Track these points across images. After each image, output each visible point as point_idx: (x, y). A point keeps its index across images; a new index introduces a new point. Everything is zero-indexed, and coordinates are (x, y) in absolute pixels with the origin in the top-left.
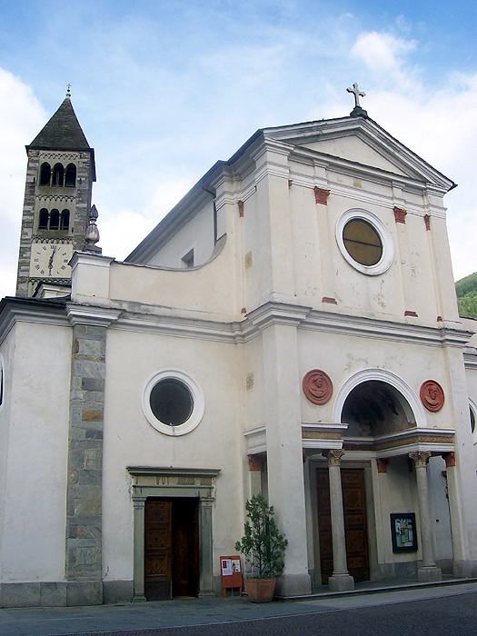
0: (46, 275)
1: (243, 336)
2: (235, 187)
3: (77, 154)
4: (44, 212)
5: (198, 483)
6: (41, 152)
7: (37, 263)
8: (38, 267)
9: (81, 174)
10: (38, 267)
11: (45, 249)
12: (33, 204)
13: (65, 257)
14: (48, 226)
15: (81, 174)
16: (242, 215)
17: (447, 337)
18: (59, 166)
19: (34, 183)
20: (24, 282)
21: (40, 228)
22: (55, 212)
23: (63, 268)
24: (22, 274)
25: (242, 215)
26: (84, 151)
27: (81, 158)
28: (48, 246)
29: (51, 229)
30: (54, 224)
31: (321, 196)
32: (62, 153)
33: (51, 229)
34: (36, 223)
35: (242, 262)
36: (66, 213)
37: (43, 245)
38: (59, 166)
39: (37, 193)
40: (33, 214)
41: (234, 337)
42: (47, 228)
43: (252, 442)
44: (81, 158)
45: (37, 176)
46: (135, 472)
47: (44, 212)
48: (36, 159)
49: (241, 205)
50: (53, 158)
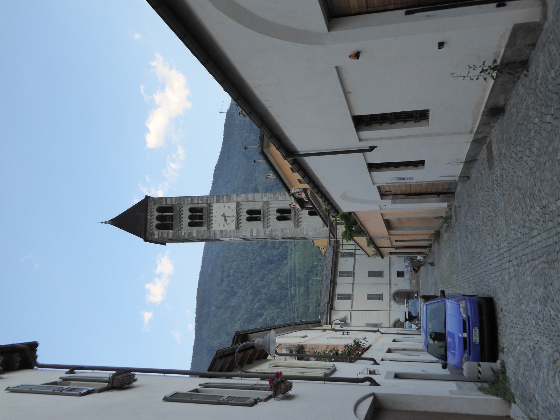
0: (234, 219)
4: (191, 225)
11: (216, 221)
13: (222, 207)
18: (158, 218)
22: (190, 217)
23: (229, 207)
28: (214, 219)
30: (201, 217)
36: (191, 210)
37: (214, 222)
38: (158, 218)
47: (191, 225)
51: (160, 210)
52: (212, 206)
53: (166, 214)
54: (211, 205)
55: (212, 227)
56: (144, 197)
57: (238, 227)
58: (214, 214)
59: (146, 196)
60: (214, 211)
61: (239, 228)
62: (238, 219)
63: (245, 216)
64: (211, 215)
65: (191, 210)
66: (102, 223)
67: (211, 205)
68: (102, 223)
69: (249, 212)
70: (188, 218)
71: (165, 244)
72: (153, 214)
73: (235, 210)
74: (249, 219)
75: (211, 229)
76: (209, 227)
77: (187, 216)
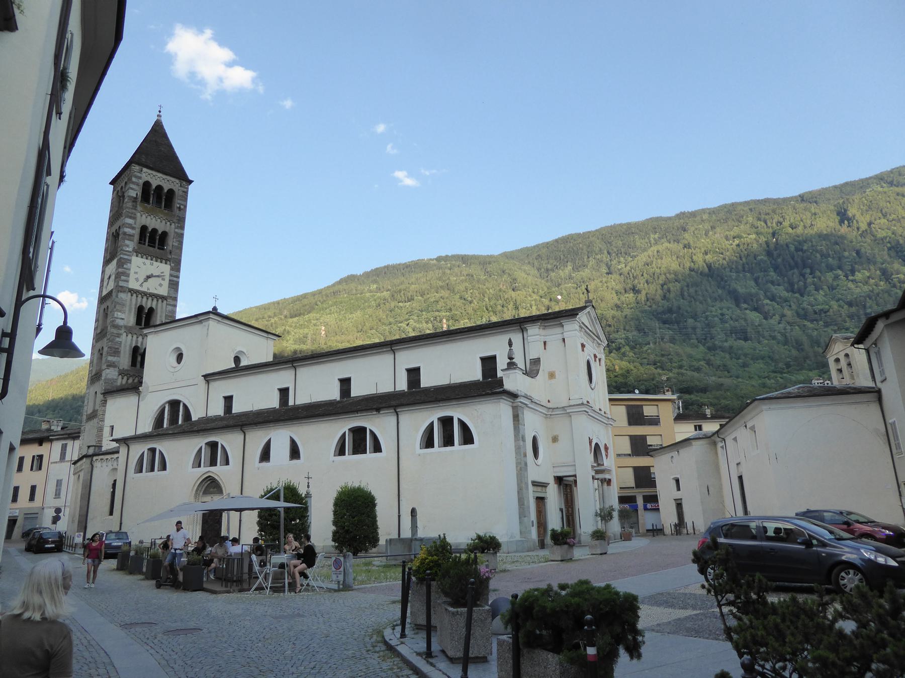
1: (551, 415)
2: (542, 332)
3: (177, 181)
4: (144, 228)
5: (544, 488)
6: (145, 170)
7: (136, 276)
8: (137, 280)
9: (179, 201)
10: (137, 280)
11: (144, 264)
12: (134, 218)
14: (147, 244)
15: (179, 201)
16: (545, 349)
17: (610, 423)
18: (159, 188)
19: (136, 198)
20: (124, 292)
21: (139, 243)
22: (154, 231)
23: (161, 285)
24: (121, 284)
25: (545, 349)
26: (183, 180)
27: (181, 186)
28: (148, 262)
29: (149, 245)
30: (152, 243)
31: (583, 346)
32: (164, 177)
33: (149, 245)
34: (137, 238)
35: (547, 376)
36: (165, 234)
37: (144, 260)
39: (139, 208)
40: (133, 228)
41: (546, 415)
42: (144, 244)
43: (556, 469)
44: (181, 186)
45: (134, 191)
46: (535, 484)
47: (144, 228)
48: (139, 175)
49: (545, 343)
50: (156, 179)
51: (171, 192)
52: (166, 263)
53: (163, 200)
54: (168, 262)
55: (137, 256)
56: (190, 178)
57: (132, 291)
58: (155, 263)
59: (190, 182)
60: (158, 264)
61: (130, 292)
62: (144, 294)
63: (148, 304)
64: (154, 259)
65: (165, 234)
66: (160, 112)
67: (168, 262)
68: (160, 112)
69: (151, 310)
70: (156, 228)
71: (111, 183)
72: (167, 183)
73: (155, 292)
74: (140, 309)
75: (135, 254)
76: (137, 252)
77: (157, 227)
